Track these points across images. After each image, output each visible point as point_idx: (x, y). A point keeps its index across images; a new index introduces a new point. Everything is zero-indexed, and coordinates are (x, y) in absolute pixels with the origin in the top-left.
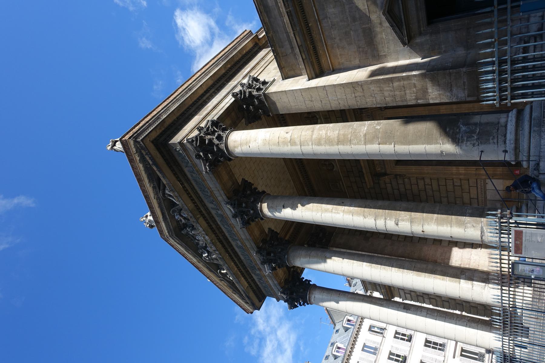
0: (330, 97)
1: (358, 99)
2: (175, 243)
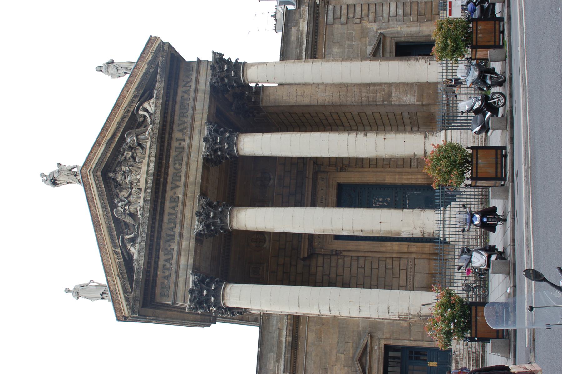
0: (319, 94)
1: (341, 97)
2: (93, 182)
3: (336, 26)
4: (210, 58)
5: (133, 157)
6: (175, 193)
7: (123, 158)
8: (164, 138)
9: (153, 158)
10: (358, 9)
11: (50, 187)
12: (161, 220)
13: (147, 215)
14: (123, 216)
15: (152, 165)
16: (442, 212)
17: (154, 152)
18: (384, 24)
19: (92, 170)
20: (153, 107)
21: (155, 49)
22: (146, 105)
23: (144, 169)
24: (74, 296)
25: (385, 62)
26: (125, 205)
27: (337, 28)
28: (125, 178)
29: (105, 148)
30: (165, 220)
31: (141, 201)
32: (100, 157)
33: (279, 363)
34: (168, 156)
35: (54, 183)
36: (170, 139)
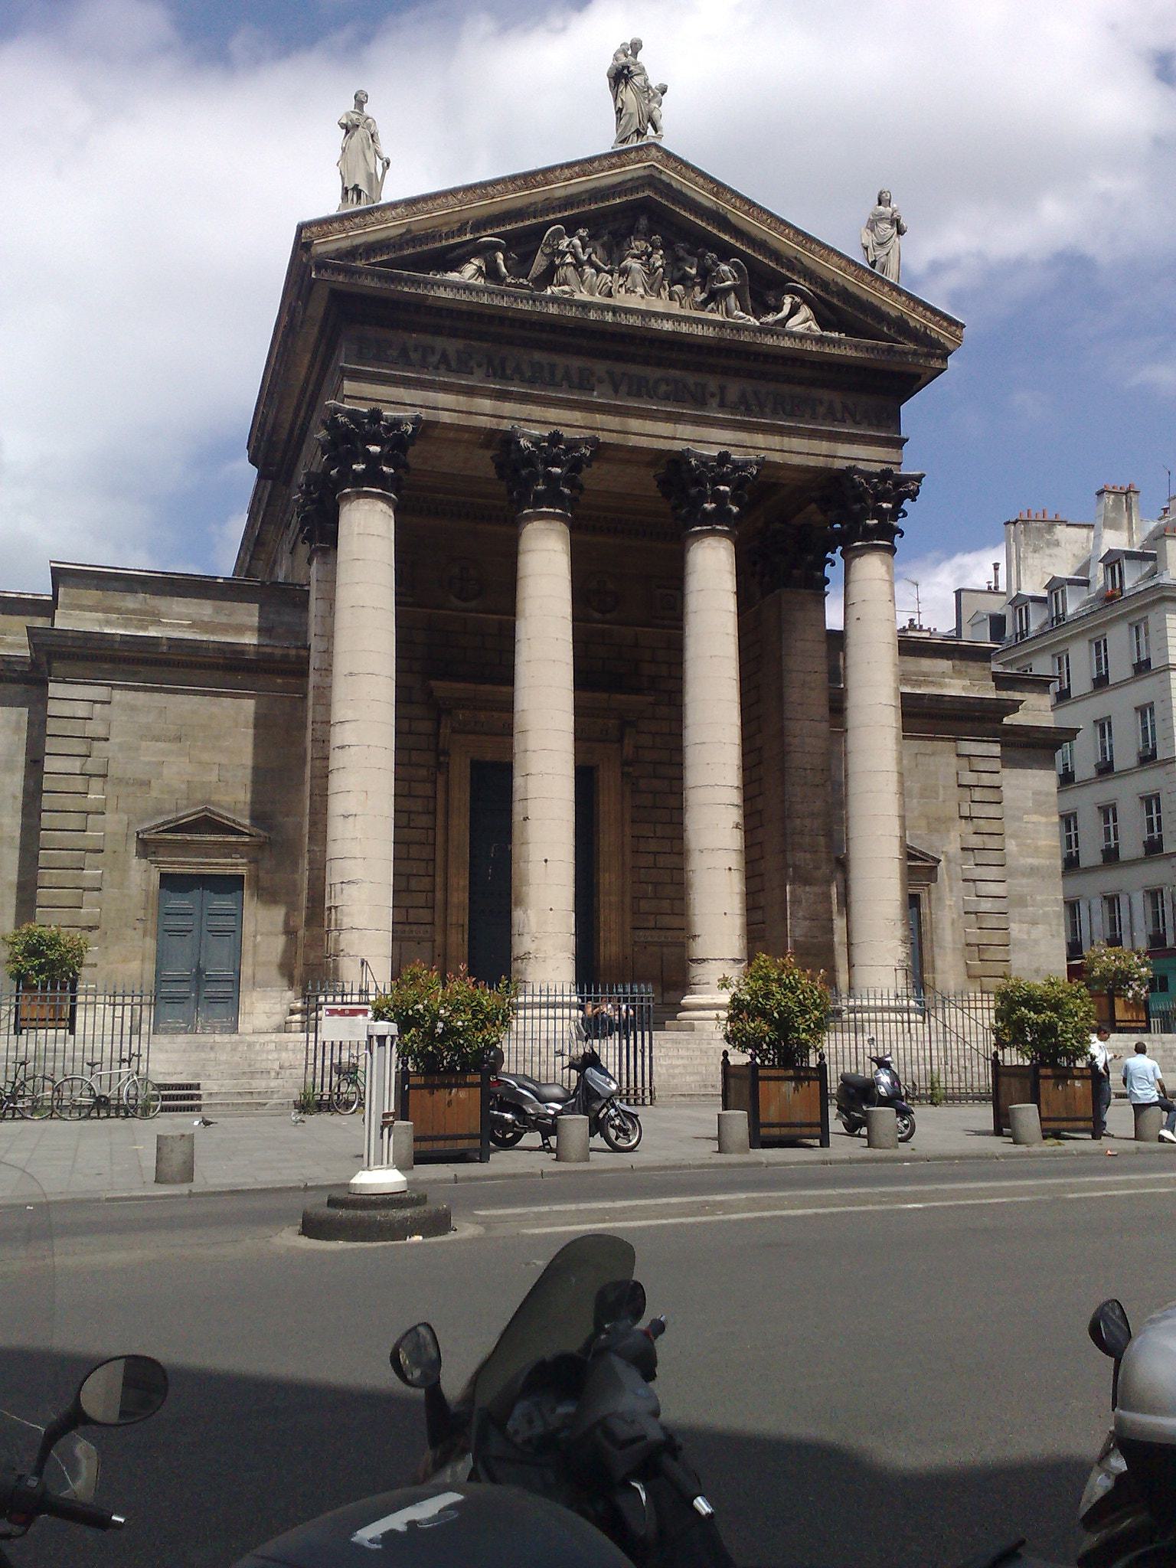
2: (629, 176)
3: (954, 760)
4: (904, 471)
5: (683, 279)
6: (601, 381)
7: (682, 253)
9: (684, 328)
10: (991, 811)
11: (607, 63)
12: (538, 345)
13: (553, 309)
14: (548, 250)
15: (668, 326)
16: (567, 999)
17: (698, 330)
18: (958, 869)
19: (657, 174)
20: (800, 329)
21: (933, 335)
22: (805, 312)
23: (659, 305)
24: (347, 115)
25: (898, 870)
26: (575, 255)
27: (948, 764)
28: (634, 256)
29: (707, 208)
30: (538, 356)
31: (583, 296)
32: (685, 195)
33: (189, 626)
34: (686, 366)
35: (620, 76)
36: (726, 372)
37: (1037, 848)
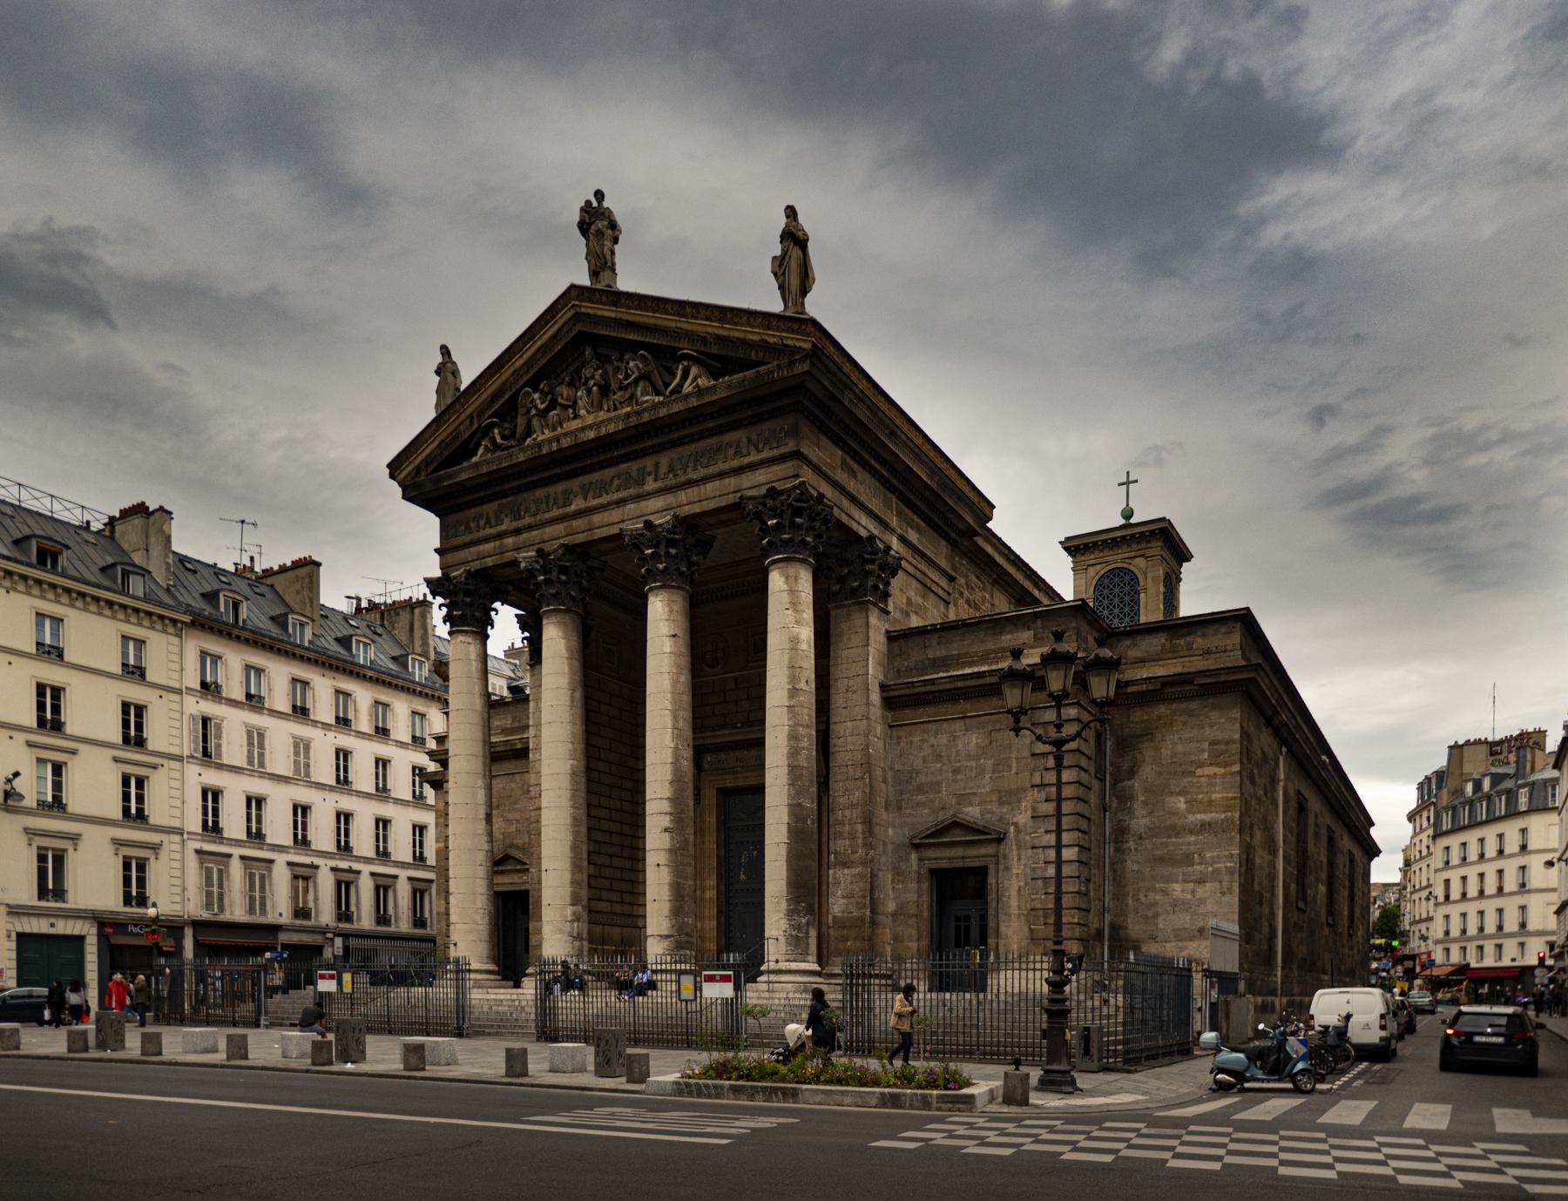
8: (650, 437)
37: (1210, 802)
